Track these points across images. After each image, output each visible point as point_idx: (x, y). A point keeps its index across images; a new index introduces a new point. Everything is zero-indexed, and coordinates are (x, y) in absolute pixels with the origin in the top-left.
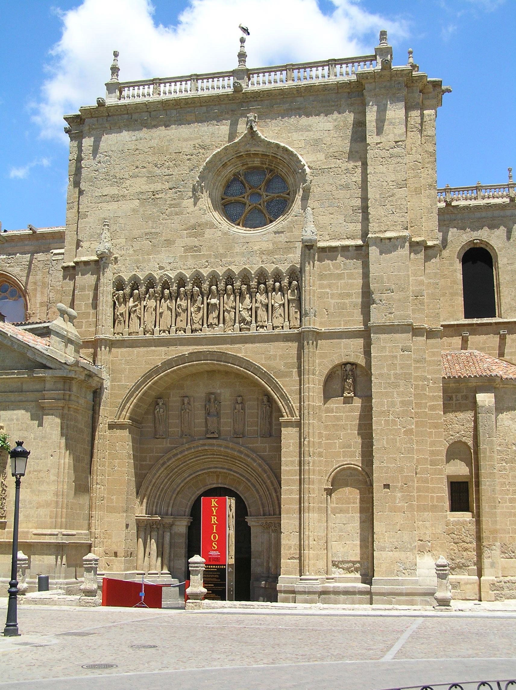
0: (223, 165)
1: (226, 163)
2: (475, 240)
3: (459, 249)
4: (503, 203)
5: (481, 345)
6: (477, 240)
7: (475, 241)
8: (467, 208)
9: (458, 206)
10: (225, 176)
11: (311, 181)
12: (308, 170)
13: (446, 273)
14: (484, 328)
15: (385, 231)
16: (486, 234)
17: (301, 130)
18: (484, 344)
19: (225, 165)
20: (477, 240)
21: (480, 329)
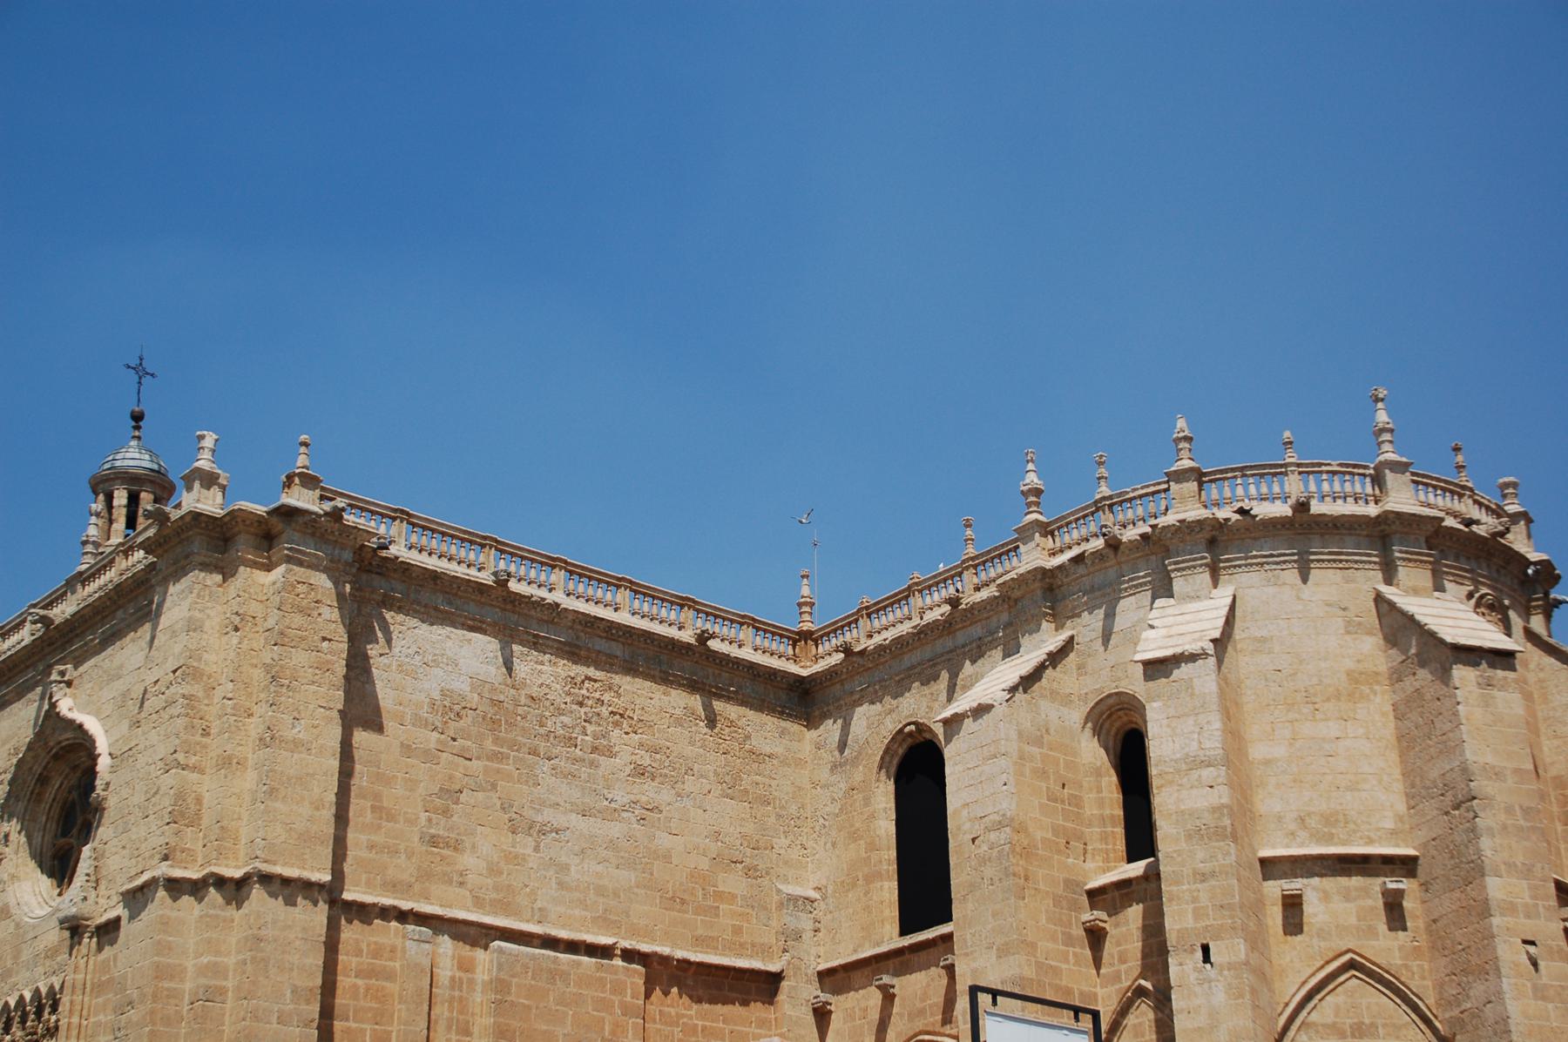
0: (38, 780)
1: (40, 774)
2: (905, 726)
3: (878, 758)
4: (942, 615)
5: (919, 1005)
6: (909, 724)
7: (907, 729)
8: (881, 649)
9: (866, 648)
10: (50, 800)
11: (108, 784)
12: (103, 763)
13: (857, 825)
14: (923, 955)
15: (142, 872)
16: (925, 704)
17: (111, 680)
18: (925, 1001)
19: (43, 780)
20: (909, 724)
21: (916, 959)
